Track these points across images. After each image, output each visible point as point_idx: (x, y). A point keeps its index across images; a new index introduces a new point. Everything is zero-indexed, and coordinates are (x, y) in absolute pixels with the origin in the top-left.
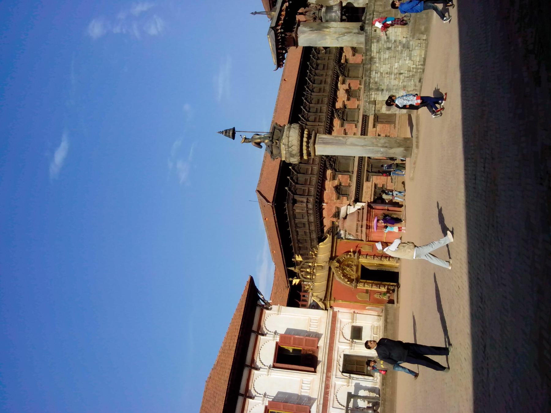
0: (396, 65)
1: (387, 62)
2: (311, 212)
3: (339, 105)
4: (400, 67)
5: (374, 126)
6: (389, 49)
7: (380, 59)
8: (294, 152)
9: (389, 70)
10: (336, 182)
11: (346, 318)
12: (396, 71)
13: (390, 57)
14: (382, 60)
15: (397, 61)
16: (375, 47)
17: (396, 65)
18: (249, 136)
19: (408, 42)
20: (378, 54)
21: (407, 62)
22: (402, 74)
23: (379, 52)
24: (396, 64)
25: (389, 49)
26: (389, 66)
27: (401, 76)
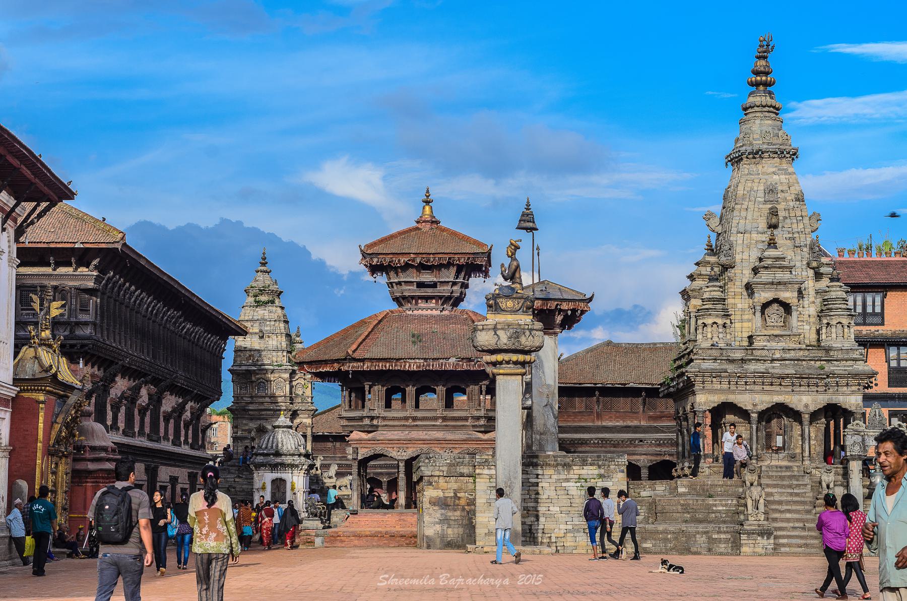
0: (555, 509)
1: (559, 492)
7: (567, 480)
8: (523, 339)
9: (544, 497)
13: (571, 498)
14: (564, 484)
15: (563, 509)
16: (590, 472)
18: (524, 256)
20: (577, 477)
21: (563, 527)
22: (538, 520)
24: (558, 509)
26: (553, 494)
27: (533, 519)
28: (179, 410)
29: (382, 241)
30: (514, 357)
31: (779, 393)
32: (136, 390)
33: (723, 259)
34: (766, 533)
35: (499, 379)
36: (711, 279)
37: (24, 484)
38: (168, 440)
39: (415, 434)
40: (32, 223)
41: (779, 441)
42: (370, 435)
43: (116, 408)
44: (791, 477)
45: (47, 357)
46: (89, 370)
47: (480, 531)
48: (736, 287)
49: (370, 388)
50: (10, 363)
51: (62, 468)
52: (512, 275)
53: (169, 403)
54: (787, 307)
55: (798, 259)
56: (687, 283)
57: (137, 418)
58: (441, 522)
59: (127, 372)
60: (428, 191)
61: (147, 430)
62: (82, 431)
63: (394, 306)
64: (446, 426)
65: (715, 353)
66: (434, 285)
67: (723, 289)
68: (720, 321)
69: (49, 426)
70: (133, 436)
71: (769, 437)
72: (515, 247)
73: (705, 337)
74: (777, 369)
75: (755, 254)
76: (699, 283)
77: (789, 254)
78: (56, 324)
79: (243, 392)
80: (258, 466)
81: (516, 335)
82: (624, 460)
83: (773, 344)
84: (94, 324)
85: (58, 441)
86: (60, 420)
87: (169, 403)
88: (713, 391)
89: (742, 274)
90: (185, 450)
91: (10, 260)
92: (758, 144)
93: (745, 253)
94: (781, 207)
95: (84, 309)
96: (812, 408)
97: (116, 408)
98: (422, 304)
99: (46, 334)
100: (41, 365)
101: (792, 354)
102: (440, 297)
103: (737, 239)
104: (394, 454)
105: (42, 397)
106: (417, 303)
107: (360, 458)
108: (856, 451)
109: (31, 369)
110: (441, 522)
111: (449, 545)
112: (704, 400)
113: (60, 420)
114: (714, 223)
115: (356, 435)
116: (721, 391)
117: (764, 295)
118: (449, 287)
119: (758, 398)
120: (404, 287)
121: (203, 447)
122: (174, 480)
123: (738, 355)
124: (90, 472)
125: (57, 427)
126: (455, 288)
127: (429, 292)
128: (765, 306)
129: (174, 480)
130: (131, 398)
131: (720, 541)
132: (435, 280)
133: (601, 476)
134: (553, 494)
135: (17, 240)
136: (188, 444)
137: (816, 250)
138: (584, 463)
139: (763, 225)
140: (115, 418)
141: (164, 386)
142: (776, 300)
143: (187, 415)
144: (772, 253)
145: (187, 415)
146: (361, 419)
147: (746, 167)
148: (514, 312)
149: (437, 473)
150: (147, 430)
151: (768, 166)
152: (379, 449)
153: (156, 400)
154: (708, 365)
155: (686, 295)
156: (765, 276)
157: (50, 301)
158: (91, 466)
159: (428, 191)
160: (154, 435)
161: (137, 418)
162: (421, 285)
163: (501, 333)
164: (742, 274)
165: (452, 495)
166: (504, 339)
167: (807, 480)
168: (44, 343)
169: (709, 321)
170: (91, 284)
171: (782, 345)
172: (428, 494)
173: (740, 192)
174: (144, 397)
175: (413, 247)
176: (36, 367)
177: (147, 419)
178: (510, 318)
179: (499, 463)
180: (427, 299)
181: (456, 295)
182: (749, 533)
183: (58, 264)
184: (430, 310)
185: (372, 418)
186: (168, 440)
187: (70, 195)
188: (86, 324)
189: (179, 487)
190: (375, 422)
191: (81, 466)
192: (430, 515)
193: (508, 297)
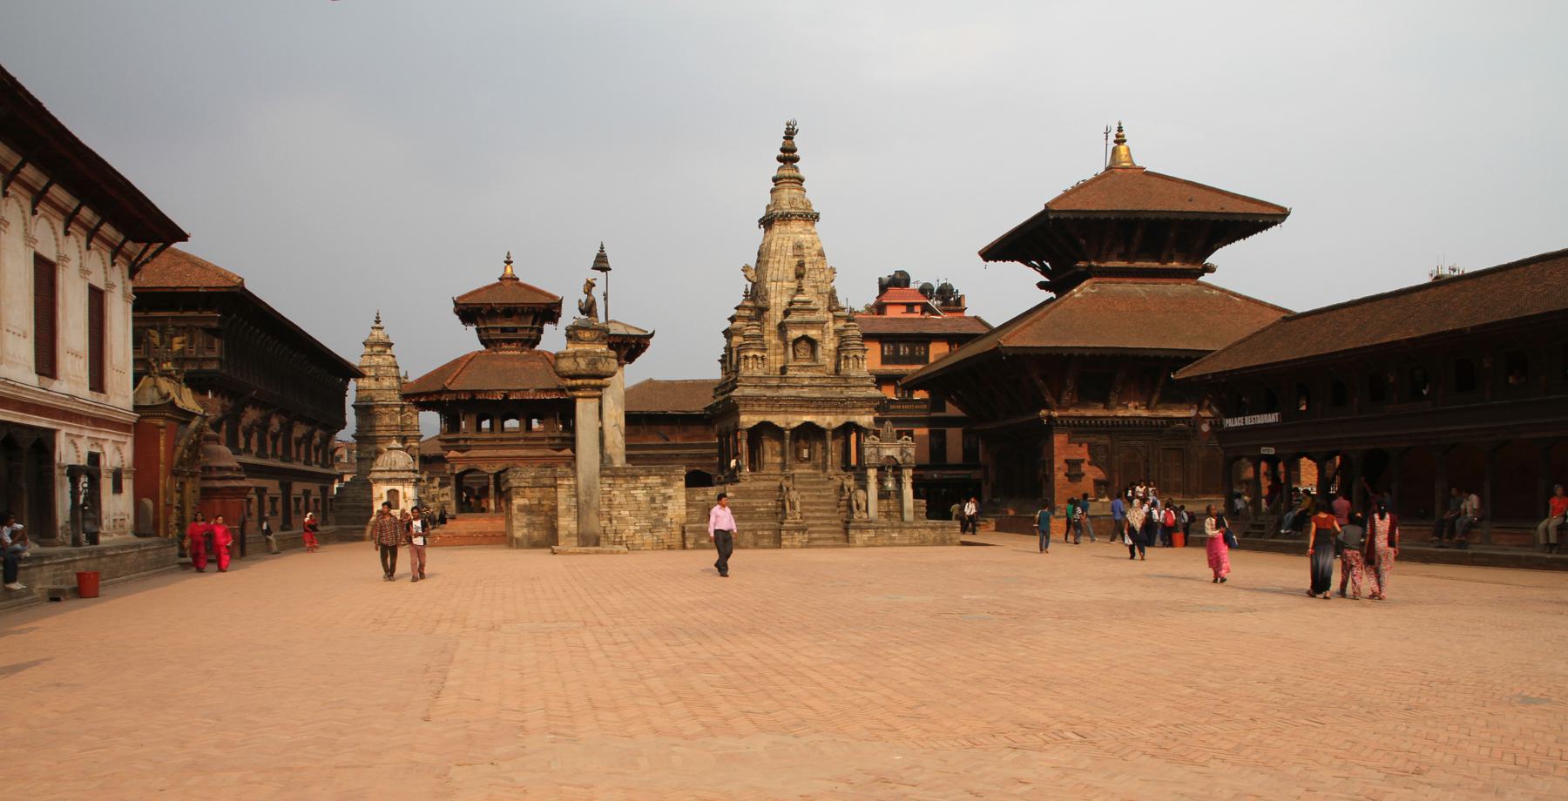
0: (625, 513)
4: (621, 519)
6: (653, 500)
8: (600, 366)
11: (117, 453)
12: (615, 513)
17: (625, 513)
18: (597, 293)
19: (665, 525)
23: (645, 487)
25: (653, 500)
26: (623, 500)
28: (309, 438)
29: (471, 294)
30: (593, 382)
31: (808, 413)
32: (267, 419)
33: (760, 303)
34: (803, 530)
35: (580, 403)
36: (750, 319)
37: (149, 503)
39: (502, 453)
40: (147, 261)
41: (805, 453)
43: (248, 434)
44: (818, 483)
45: (166, 386)
46: (218, 401)
47: (562, 533)
48: (771, 327)
50: (131, 392)
51: (188, 487)
52: (588, 309)
53: (299, 431)
54: (812, 343)
55: (821, 303)
56: (728, 324)
57: (269, 443)
58: (528, 526)
59: (256, 403)
61: (280, 453)
62: (208, 453)
63: (482, 348)
65: (755, 381)
66: (515, 330)
67: (761, 328)
68: (759, 354)
69: (172, 448)
70: (266, 457)
71: (798, 451)
72: (590, 286)
73: (747, 367)
74: (806, 393)
75: (786, 300)
76: (738, 324)
77: (815, 300)
78: (180, 360)
80: (377, 481)
81: (593, 362)
82: (683, 471)
83: (803, 374)
84: (220, 360)
85: (181, 462)
86: (182, 443)
87: (299, 431)
88: (753, 412)
89: (776, 316)
90: (316, 469)
91: (125, 295)
92: (786, 208)
93: (778, 300)
94: (807, 260)
95: (211, 348)
96: (834, 426)
97: (248, 434)
99: (167, 366)
100: (160, 393)
101: (818, 382)
103: (771, 286)
104: (485, 469)
105: (161, 423)
108: (873, 460)
109: (151, 397)
110: (528, 526)
111: (535, 545)
112: (748, 420)
113: (182, 443)
114: (751, 274)
115: (453, 454)
116: (760, 413)
117: (795, 334)
119: (790, 418)
121: (332, 466)
122: (307, 493)
123: (774, 383)
124: (216, 490)
125: (180, 449)
127: (511, 336)
128: (796, 341)
129: (307, 493)
130: (263, 426)
131: (763, 537)
133: (663, 484)
134: (623, 500)
135: (132, 275)
137: (832, 295)
138: (649, 475)
139: (792, 275)
140: (248, 443)
141: (292, 417)
142: (805, 338)
143: (317, 440)
144: (799, 298)
145: (317, 440)
146: (457, 440)
147: (777, 228)
148: (591, 342)
150: (280, 453)
151: (796, 227)
152: (472, 465)
153: (287, 429)
154: (749, 391)
155: (728, 334)
156: (794, 317)
157: (172, 337)
158: (218, 484)
160: (286, 456)
161: (269, 443)
162: (504, 330)
163: (580, 360)
164: (776, 316)
166: (583, 364)
167: (831, 485)
168: (166, 374)
169: (751, 354)
170: (215, 325)
171: (809, 374)
172: (518, 501)
173: (773, 248)
174: (275, 424)
175: (496, 299)
176: (156, 395)
177: (280, 444)
178: (588, 347)
179: (580, 476)
180: (509, 342)
182: (788, 530)
183: (187, 308)
184: (512, 351)
187: (183, 237)
188: (212, 360)
189: (311, 499)
191: (209, 484)
193: (586, 329)
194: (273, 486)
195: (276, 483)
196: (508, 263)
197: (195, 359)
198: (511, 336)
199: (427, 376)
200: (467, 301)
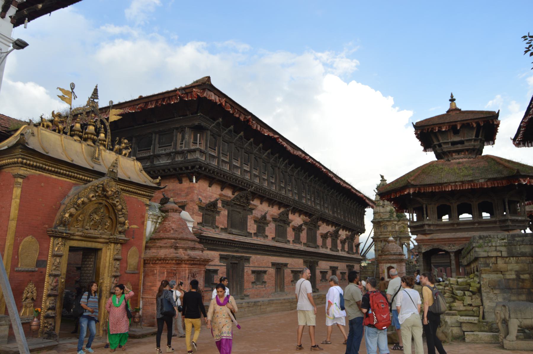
2: (179, 159)
3: (291, 216)
5: (273, 264)
10: (220, 205)
38: (327, 248)
39: (459, 235)
42: (428, 237)
49: (426, 206)
60: (452, 95)
64: (482, 228)
66: (462, 142)
79: (378, 230)
98: (455, 156)
102: (467, 150)
104: (446, 248)
106: (452, 156)
107: (423, 251)
118: (473, 143)
120: (444, 146)
126: (476, 143)
127: (460, 147)
132: (462, 139)
136: (345, 251)
146: (423, 226)
149: (494, 254)
152: (436, 245)
159: (452, 95)
162: (454, 143)
165: (514, 276)
177: (304, 235)
180: (458, 152)
181: (477, 147)
185: (429, 225)
186: (327, 248)
188: (194, 151)
190: (432, 228)
192: (491, 300)
194: (297, 263)
195: (301, 261)
196: (452, 100)
197: (182, 153)
198: (460, 147)
199: (397, 181)
200: (423, 124)
